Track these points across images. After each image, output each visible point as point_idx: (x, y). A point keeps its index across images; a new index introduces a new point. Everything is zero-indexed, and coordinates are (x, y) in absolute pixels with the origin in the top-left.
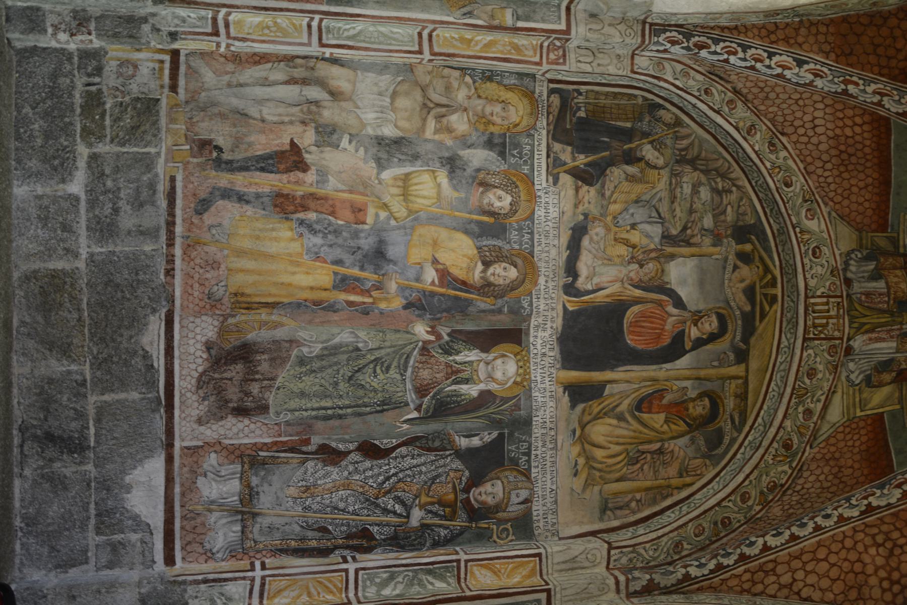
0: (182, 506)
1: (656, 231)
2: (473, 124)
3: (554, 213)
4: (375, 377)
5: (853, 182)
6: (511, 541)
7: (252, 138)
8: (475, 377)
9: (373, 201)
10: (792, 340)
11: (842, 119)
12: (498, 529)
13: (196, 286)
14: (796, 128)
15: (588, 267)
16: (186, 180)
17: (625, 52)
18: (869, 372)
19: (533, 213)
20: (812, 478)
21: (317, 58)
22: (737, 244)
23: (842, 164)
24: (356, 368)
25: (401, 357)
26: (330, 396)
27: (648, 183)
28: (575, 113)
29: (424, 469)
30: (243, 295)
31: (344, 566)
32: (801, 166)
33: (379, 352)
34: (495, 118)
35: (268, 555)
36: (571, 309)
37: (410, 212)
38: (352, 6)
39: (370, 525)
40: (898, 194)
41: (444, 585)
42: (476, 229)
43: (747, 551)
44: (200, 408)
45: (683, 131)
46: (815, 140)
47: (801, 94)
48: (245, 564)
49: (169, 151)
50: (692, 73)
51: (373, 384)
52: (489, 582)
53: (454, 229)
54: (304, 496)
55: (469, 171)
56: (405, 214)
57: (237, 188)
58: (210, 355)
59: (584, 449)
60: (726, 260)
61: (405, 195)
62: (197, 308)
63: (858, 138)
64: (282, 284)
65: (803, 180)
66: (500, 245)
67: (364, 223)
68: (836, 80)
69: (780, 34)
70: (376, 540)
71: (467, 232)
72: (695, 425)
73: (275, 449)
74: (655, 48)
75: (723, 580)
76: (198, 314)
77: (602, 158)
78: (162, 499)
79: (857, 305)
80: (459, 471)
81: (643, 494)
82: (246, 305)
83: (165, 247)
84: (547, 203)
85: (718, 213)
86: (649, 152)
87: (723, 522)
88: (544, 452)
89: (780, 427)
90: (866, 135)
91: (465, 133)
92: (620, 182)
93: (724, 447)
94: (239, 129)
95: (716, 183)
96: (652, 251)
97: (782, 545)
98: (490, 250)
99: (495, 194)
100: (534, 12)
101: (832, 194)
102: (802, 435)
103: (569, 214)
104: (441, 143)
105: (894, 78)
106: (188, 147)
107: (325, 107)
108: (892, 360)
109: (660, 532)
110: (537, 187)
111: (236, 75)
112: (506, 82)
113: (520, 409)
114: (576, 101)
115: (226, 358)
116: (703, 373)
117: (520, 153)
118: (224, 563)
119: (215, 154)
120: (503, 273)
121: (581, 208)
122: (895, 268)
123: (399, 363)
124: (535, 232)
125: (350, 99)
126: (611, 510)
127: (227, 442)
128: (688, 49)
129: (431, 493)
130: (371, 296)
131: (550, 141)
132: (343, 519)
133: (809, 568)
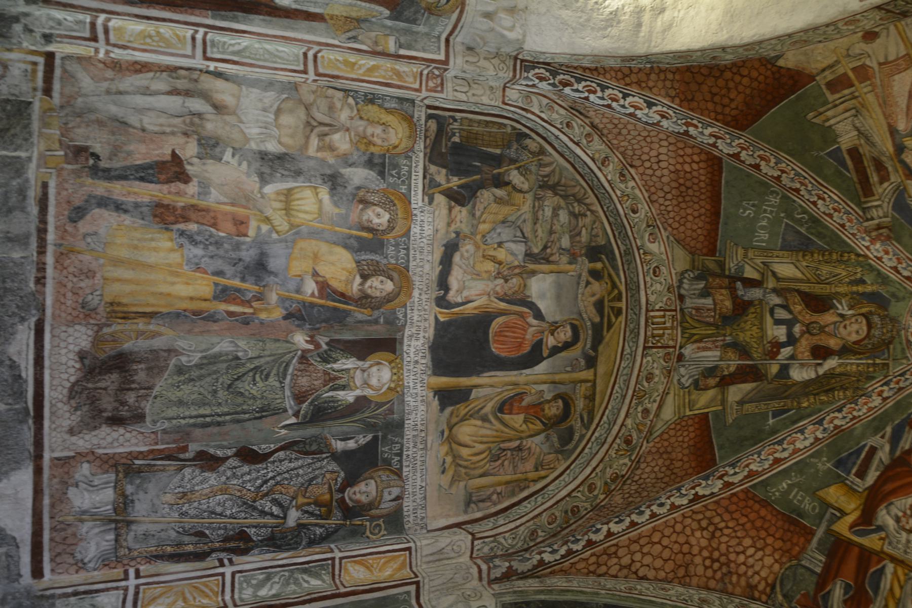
0: (52, 518)
1: (520, 249)
2: (355, 145)
3: (428, 230)
4: (255, 384)
5: (689, 211)
7: (132, 147)
8: (352, 384)
9: (255, 215)
10: (634, 349)
11: (682, 156)
13: (69, 295)
14: (643, 161)
15: (458, 281)
16: (60, 187)
17: (498, 85)
18: (696, 377)
19: (409, 230)
20: (648, 470)
21: (201, 71)
22: (590, 262)
23: (680, 196)
24: (235, 377)
26: (208, 404)
27: (513, 205)
28: (450, 138)
29: (301, 472)
30: (119, 304)
31: (221, 570)
32: (646, 195)
33: (258, 360)
34: (375, 139)
35: (143, 562)
36: (442, 320)
37: (292, 226)
38: (238, 22)
40: (726, 224)
41: (319, 582)
42: (355, 244)
43: (594, 537)
45: (547, 159)
46: (658, 173)
47: (649, 132)
48: (118, 572)
49: (41, 156)
50: (556, 107)
51: (252, 391)
52: (362, 577)
53: (334, 243)
54: (181, 502)
55: (350, 189)
56: (287, 228)
57: (115, 197)
58: (83, 364)
59: (451, 448)
60: (580, 276)
61: (288, 210)
62: (69, 318)
63: (695, 174)
64: (161, 294)
65: (647, 208)
66: (378, 259)
67: (246, 235)
68: (679, 122)
69: (634, 78)
70: (253, 541)
71: (346, 247)
72: (550, 424)
73: (151, 457)
74: (524, 83)
75: (572, 564)
76: (71, 323)
77: (474, 181)
78: (30, 512)
79: (688, 318)
81: (504, 487)
82: (123, 315)
83: (35, 254)
84: (422, 221)
85: (575, 235)
86: (515, 177)
87: (572, 511)
88: (415, 452)
89: (623, 425)
90: (701, 171)
92: (489, 204)
93: (574, 442)
94: (118, 137)
95: (573, 207)
96: (516, 267)
97: (624, 530)
98: (368, 265)
99: (374, 211)
100: (416, 41)
101: (670, 221)
102: (640, 431)
103: (442, 231)
104: (323, 161)
105: (727, 124)
106: (62, 153)
108: (716, 367)
109: (518, 522)
110: (413, 206)
111: (116, 82)
112: (387, 105)
113: (393, 413)
114: (451, 127)
115: (100, 367)
116: (557, 378)
117: (398, 173)
118: (96, 573)
119: (91, 162)
120: (380, 286)
121: (453, 227)
122: (721, 288)
124: (411, 248)
125: (234, 113)
126: (474, 503)
127: (101, 451)
128: (553, 85)
130: (251, 307)
132: (220, 523)
133: (645, 550)
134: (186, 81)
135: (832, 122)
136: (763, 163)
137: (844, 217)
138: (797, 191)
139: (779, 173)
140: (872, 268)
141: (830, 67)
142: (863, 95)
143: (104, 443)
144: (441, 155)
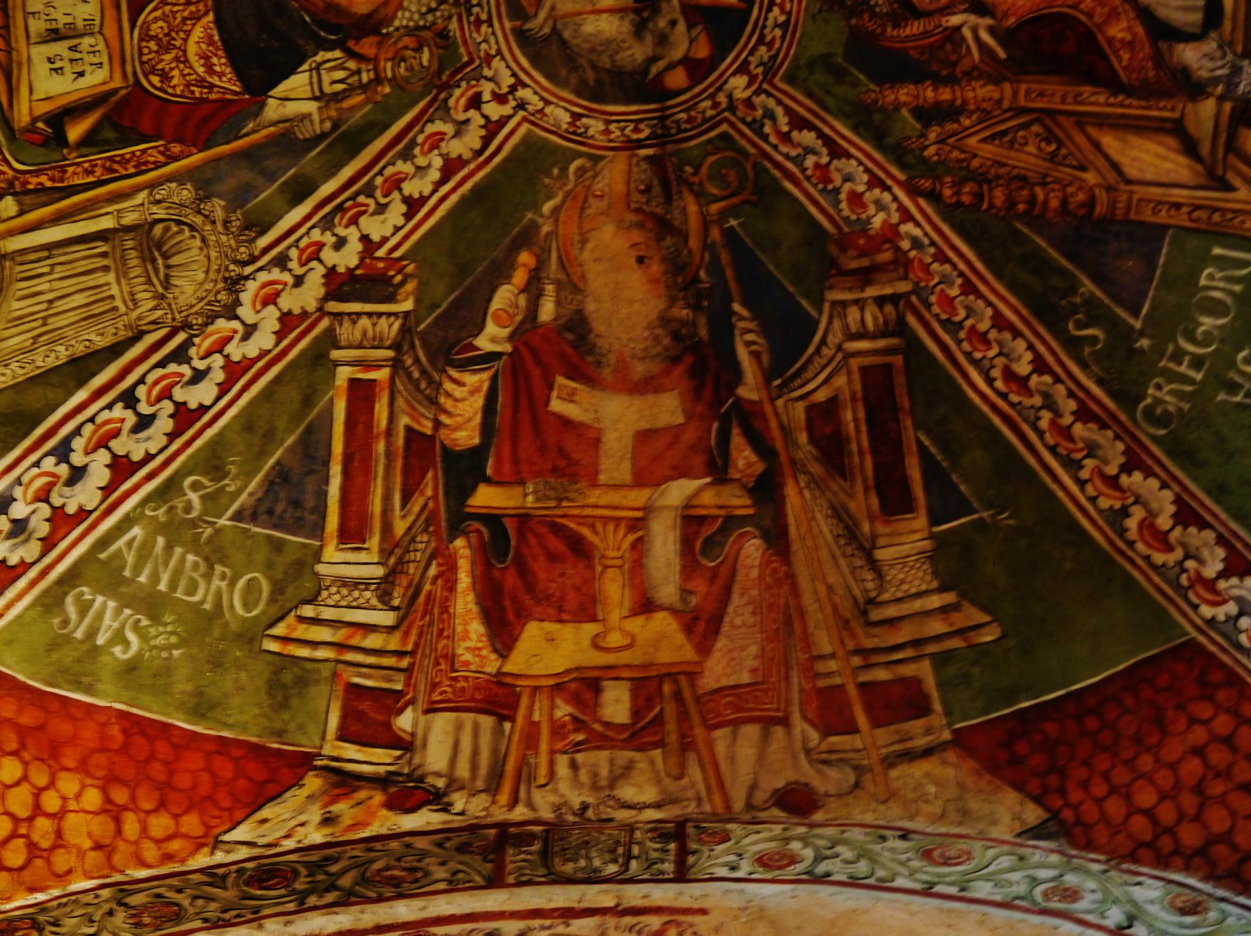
135: (936, 601)
136: (1164, 522)
137: (962, 313)
138: (1083, 414)
139: (1124, 480)
140: (899, 154)
141: (910, 756)
142: (841, 653)
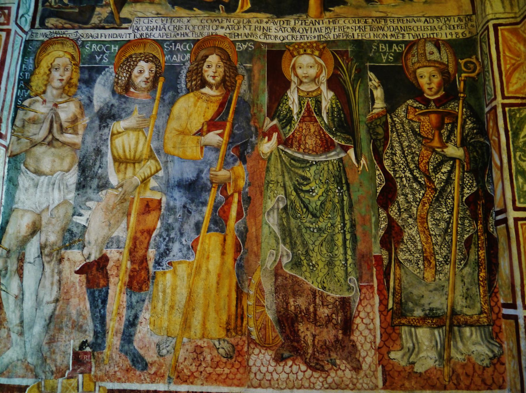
2: (71, 97)
4: (313, 191)
6: (477, 59)
7: (74, 312)
9: (139, 193)
12: (465, 72)
13: (219, 370)
19: (156, 41)
24: (305, 210)
25: (294, 166)
26: (332, 236)
29: (406, 144)
30: (228, 323)
31: (511, 222)
34: (64, 78)
35: (495, 300)
36: (249, 6)
37: (151, 156)
39: (463, 196)
42: (170, 94)
44: (343, 368)
51: (320, 193)
53: (169, 115)
55: (114, 101)
56: (153, 161)
57: (122, 327)
58: (289, 357)
61: (135, 161)
62: (241, 370)
64: (218, 283)
66: (185, 71)
67: (160, 201)
70: (477, 191)
71: (172, 103)
73: (385, 292)
76: (248, 369)
80: (407, 109)
84: (147, 29)
88: (389, 28)
91: (78, 105)
94: (64, 324)
98: (191, 81)
99: (137, 77)
103: (159, 9)
104: (86, 128)
106: (80, 376)
107: (47, 240)
110: (132, 38)
111: (11, 326)
112: (31, 67)
114: (53, 4)
115: (292, 341)
117: (99, 53)
118: (505, 346)
119: (88, 349)
123: (300, 168)
124: (175, 38)
125: (39, 215)
127: (378, 340)
129: (430, 137)
130: (232, 195)
131: (89, 26)
132: (458, 224)
134: (9, 261)
143: (370, 338)
144: (81, 12)
